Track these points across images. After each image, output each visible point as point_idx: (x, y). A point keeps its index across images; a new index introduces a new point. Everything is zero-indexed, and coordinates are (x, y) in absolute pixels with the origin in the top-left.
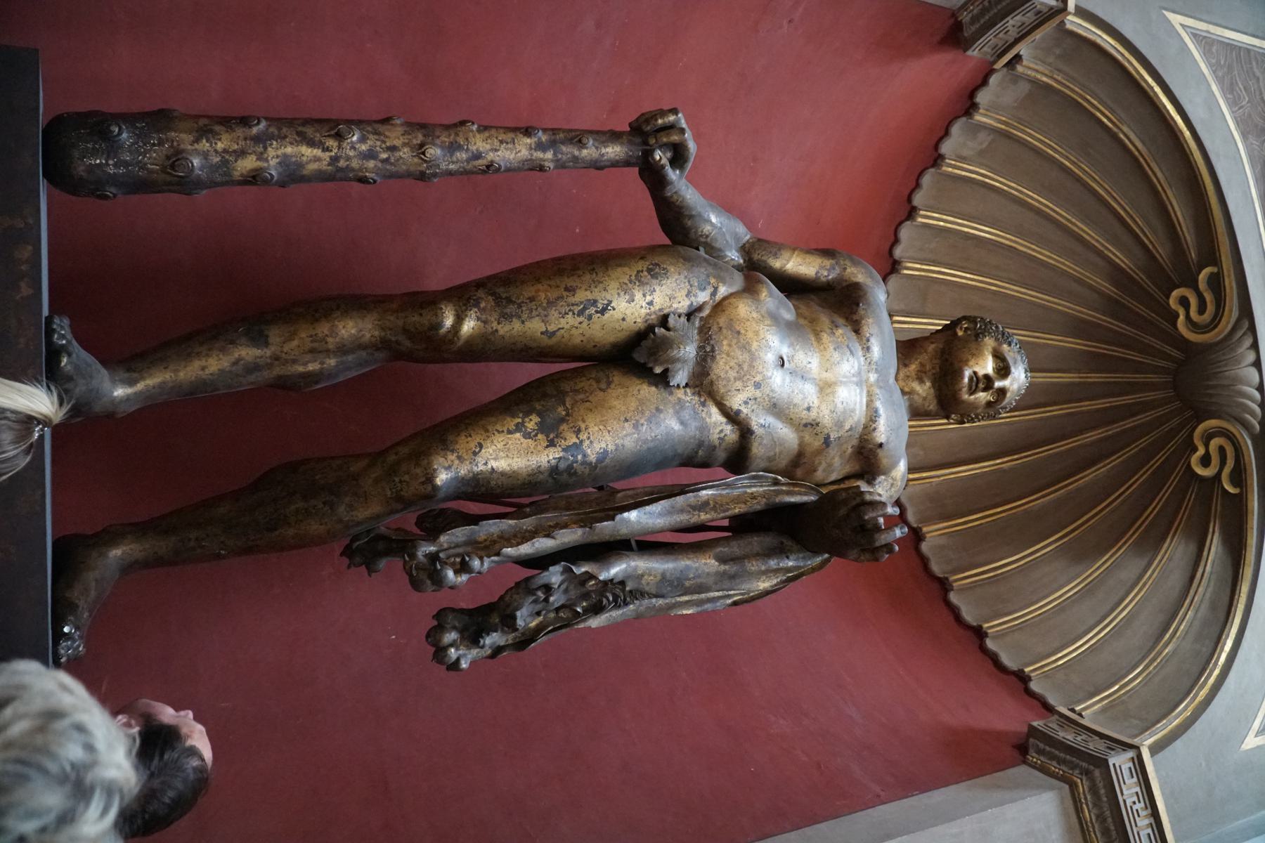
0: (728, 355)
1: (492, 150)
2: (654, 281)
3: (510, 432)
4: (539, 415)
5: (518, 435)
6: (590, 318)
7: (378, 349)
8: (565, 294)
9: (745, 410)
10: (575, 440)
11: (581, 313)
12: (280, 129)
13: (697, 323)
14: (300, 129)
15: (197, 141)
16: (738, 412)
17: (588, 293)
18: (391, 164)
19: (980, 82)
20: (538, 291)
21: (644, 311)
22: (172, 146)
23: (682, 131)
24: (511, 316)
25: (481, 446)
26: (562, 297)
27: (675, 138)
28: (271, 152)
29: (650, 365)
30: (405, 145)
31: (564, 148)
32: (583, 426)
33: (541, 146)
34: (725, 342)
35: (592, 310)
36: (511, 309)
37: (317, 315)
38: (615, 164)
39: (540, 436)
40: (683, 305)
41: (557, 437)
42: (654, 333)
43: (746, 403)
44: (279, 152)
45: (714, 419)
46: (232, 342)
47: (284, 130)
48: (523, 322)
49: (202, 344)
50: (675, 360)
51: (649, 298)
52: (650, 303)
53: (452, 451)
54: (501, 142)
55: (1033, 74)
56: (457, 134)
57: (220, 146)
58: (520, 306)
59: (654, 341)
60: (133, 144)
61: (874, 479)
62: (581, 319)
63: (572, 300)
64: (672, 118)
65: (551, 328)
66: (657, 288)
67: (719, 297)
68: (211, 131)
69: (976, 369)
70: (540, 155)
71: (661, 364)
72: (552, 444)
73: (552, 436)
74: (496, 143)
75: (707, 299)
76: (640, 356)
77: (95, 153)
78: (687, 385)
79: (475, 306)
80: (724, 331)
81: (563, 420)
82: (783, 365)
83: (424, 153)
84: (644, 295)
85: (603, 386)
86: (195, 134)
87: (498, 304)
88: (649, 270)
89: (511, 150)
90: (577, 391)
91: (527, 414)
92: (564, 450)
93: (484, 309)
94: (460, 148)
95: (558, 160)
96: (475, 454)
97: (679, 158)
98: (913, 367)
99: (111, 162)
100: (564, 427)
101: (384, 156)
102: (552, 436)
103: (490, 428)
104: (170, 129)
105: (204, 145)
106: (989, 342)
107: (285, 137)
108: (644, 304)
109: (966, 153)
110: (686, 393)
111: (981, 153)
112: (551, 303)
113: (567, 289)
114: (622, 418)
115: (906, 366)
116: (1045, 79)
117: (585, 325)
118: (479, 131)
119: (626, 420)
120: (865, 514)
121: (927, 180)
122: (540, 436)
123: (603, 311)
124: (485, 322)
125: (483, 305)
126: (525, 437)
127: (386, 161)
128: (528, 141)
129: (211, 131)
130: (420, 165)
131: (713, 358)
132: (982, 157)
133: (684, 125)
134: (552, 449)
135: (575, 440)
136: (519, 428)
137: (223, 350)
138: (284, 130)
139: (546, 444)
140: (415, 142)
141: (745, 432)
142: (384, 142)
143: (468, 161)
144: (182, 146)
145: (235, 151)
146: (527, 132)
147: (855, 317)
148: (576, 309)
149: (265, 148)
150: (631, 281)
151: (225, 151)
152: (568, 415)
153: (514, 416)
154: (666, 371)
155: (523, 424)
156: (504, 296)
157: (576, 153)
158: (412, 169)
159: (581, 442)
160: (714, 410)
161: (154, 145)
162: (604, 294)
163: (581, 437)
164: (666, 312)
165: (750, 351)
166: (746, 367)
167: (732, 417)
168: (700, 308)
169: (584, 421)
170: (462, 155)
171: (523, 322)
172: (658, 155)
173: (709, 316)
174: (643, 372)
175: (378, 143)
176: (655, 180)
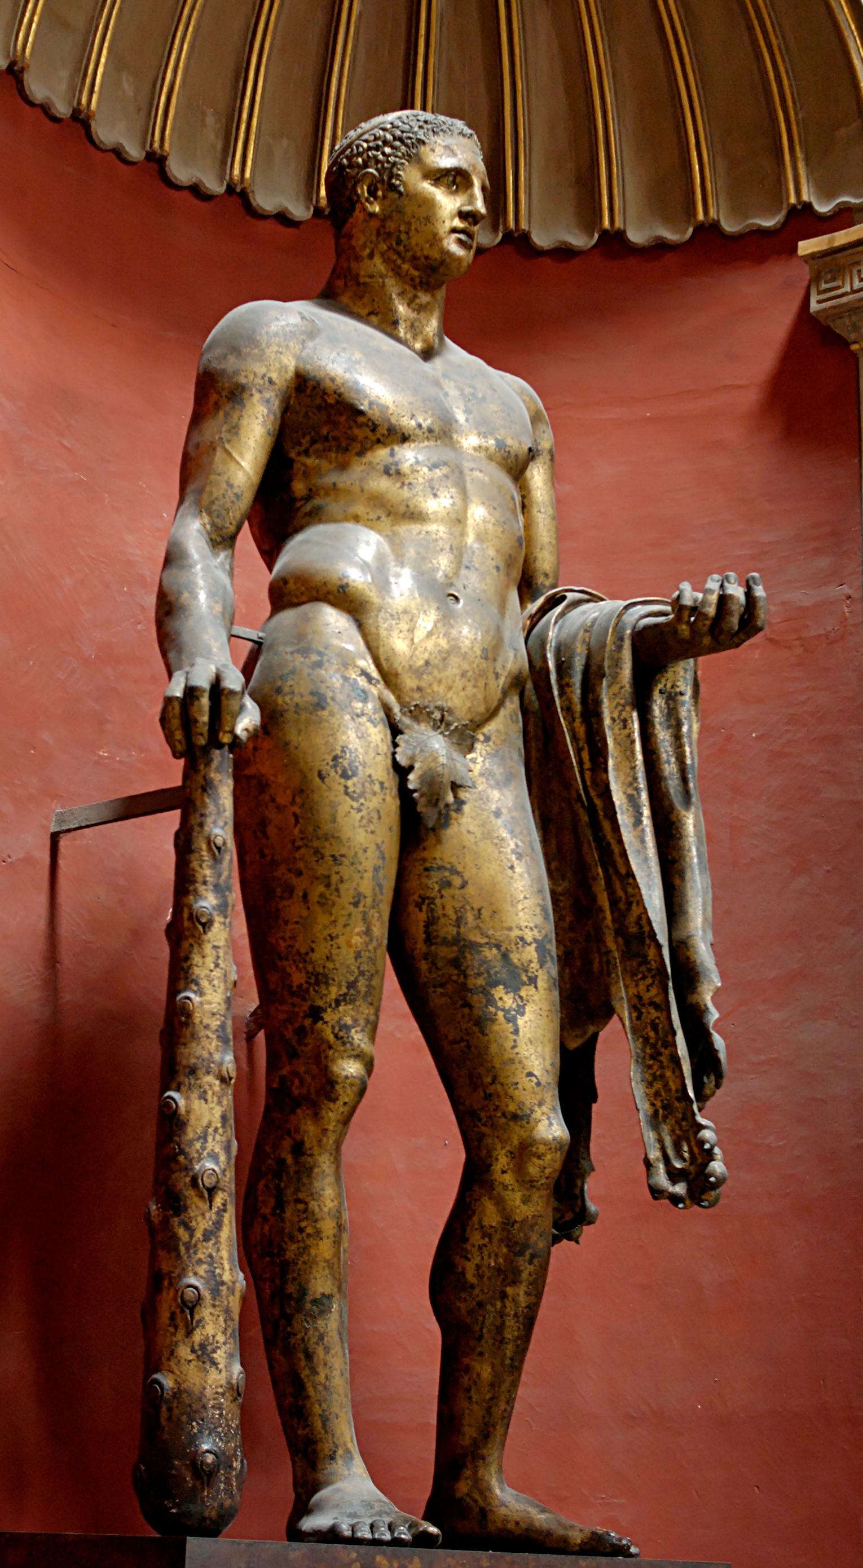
0: (450, 688)
3: (516, 1032)
4: (495, 984)
5: (521, 1021)
8: (361, 908)
9: (502, 681)
12: (200, 1262)
13: (407, 721)
14: (199, 1235)
15: (214, 1364)
20: (349, 945)
21: (388, 799)
22: (223, 1394)
25: (530, 1074)
26: (365, 913)
28: (226, 1277)
30: (220, 1103)
34: (435, 688)
37: (309, 1230)
39: (523, 993)
41: (526, 971)
42: (415, 791)
44: (227, 1266)
45: (501, 727)
46: (321, 1337)
47: (200, 1255)
49: (315, 1372)
51: (377, 788)
52: (382, 784)
53: (532, 1111)
56: (207, 1027)
57: (221, 1338)
59: (422, 796)
60: (221, 1439)
67: (375, 674)
68: (203, 1346)
72: (533, 981)
73: (525, 978)
77: (228, 1482)
80: (423, 684)
81: (505, 956)
82: (457, 598)
85: (457, 881)
86: (208, 1366)
87: (352, 1001)
88: (345, 776)
90: (459, 921)
91: (490, 1001)
93: (355, 1020)
98: (402, 309)
99: (235, 1465)
100: (514, 957)
102: (525, 978)
103: (506, 1056)
104: (202, 1394)
105: (220, 1356)
106: (411, 177)
107: (210, 1256)
113: (356, 904)
114: (510, 872)
115: (395, 323)
119: (512, 867)
120: (731, 628)
122: (523, 993)
125: (348, 1021)
126: (523, 1014)
129: (203, 1346)
131: (450, 711)
137: (327, 1350)
138: (200, 1255)
139: (532, 988)
140: (217, 1088)
142: (216, 1130)
144: (223, 1382)
145: (225, 1321)
147: (382, 431)
149: (223, 1283)
151: (224, 1332)
152: (498, 947)
153: (493, 1021)
156: (344, 990)
161: (221, 1415)
166: (466, 667)
168: (387, 710)
169: (510, 929)
173: (399, 698)
175: (218, 1137)
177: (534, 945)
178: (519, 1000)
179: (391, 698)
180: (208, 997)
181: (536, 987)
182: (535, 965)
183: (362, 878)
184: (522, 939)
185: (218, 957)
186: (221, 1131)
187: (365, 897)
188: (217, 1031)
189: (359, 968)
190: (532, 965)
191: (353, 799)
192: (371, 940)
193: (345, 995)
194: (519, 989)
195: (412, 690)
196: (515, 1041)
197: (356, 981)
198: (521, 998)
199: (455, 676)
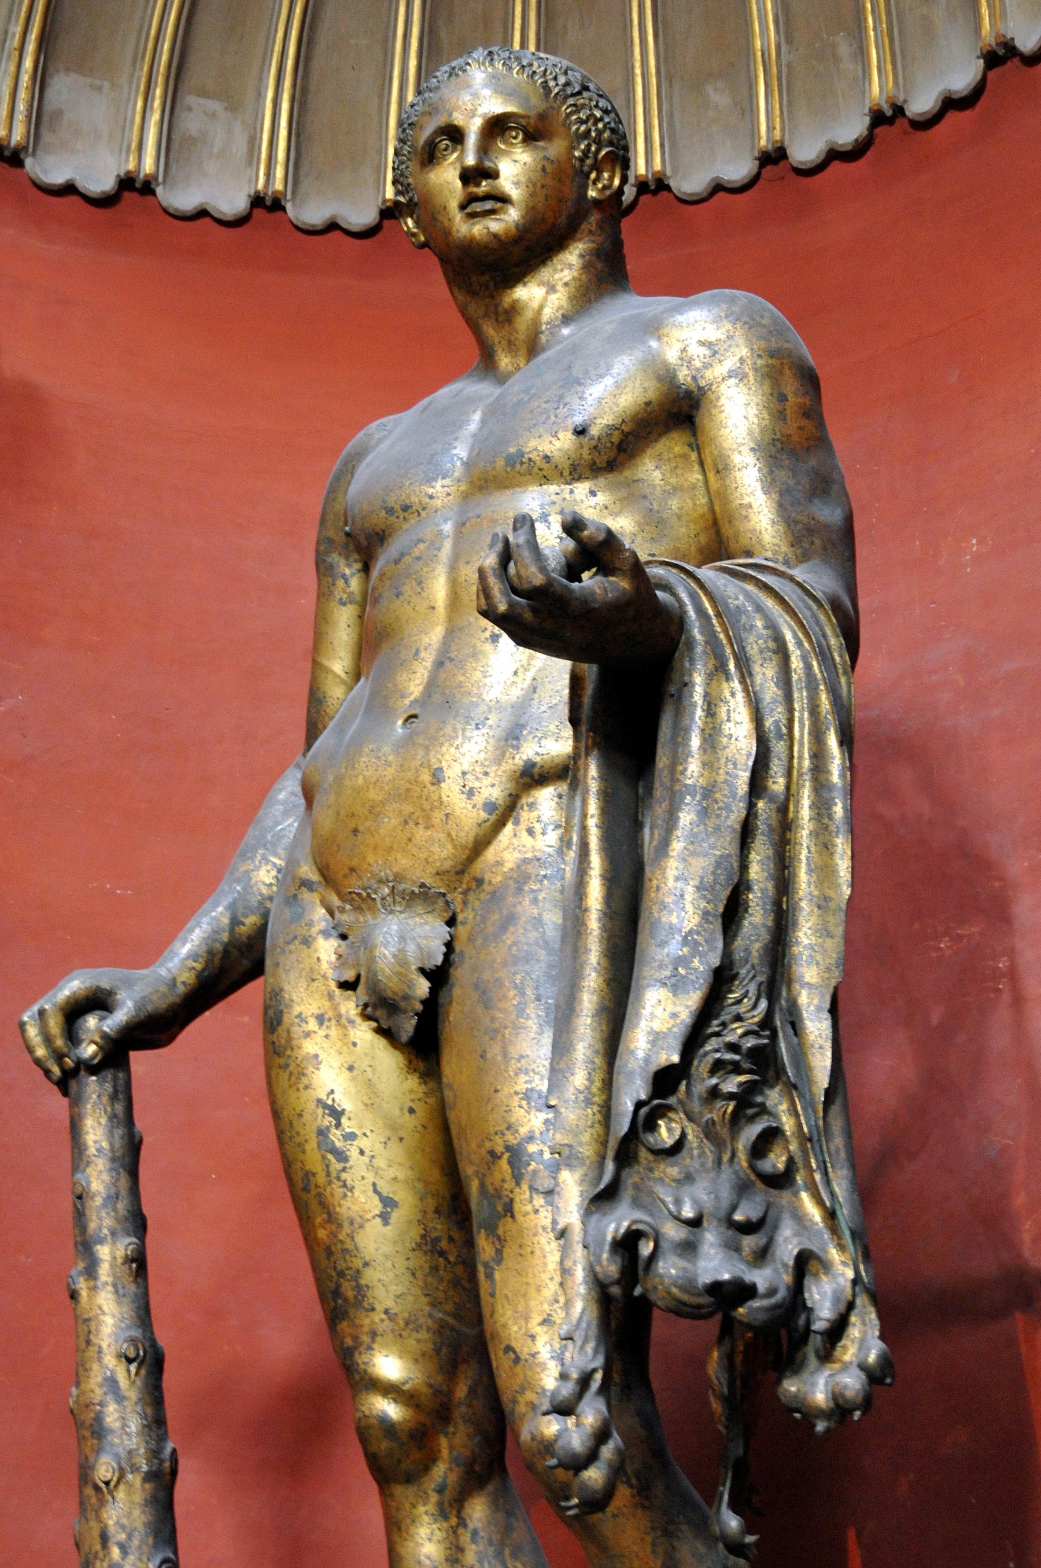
1: (100, 1359)
2: (286, 1019)
5: (497, 1275)
6: (351, 1137)
7: (462, 1523)
10: (504, 1163)
11: (342, 1156)
16: (490, 807)
17: (308, 1147)
18: (130, 1537)
19: (75, 198)
23: (42, 1013)
24: (359, 1287)
25: (509, 1349)
27: (55, 1024)
29: (419, 1007)
31: (92, 1226)
32: (488, 1145)
33: (91, 1272)
35: (336, 1137)
36: (348, 1290)
38: (125, 1120)
40: (327, 949)
41: (500, 1197)
43: (471, 793)
48: (366, 1264)
50: (401, 960)
51: (312, 1025)
52: (320, 1019)
54: (88, 1342)
55: (23, 94)
58: (341, 1274)
59: (375, 1008)
61: (689, 394)
62: (353, 1153)
63: (321, 1179)
64: (32, 1032)
65: (375, 1206)
66: (297, 1009)
69: (454, 205)
70: (104, 1272)
71: (411, 985)
72: (509, 1209)
74: (92, 1352)
75: (315, 898)
76: (408, 1026)
78: (451, 922)
79: (352, 1355)
82: (414, 716)
83: (107, 1483)
84: (307, 1035)
89: (99, 1323)
92: (518, 1184)
94: (99, 1419)
95: (113, 1234)
96: (517, 1360)
97: (98, 1001)
101: (115, 1552)
108: (322, 1033)
109: (240, 145)
110: (464, 923)
111: (234, 106)
112: (332, 1218)
116: (28, 63)
117: (363, 1143)
118: (78, 1384)
121: (311, 212)
122: (500, 1232)
123: (337, 1114)
124: (374, 1334)
127: (124, 1549)
128: (84, 1293)
130: (130, 1485)
131: (398, 878)
132: (236, 98)
133: (35, 1008)
134: (517, 1207)
135: (504, 1163)
136: (490, 1276)
141: (532, 777)
142: (97, 1553)
143: (120, 1398)
146: (74, 1295)
148: (336, 1166)
150: (287, 1066)
154: (422, 971)
155: (486, 1265)
157: (98, 1201)
158: (138, 1498)
159: (508, 1148)
160: (490, 854)
162: (307, 1117)
163: (499, 1149)
164: (333, 985)
165: (383, 803)
167: (505, 812)
170: (112, 1415)
171: (366, 1264)
172: (89, 1050)
173: (339, 894)
174: (431, 1013)
176: (155, 1029)
177: (506, 1156)
178: (497, 1242)
179: (335, 901)
180: (83, 1386)
181: (513, 1217)
182: (509, 1184)
183: (304, 1152)
184: (492, 1153)
185: (89, 1332)
186: (101, 1555)
187: (314, 1174)
188: (91, 1425)
189: (335, 1268)
190: (506, 1186)
191: (279, 1055)
192: (340, 1226)
193: (335, 1308)
194: (496, 1227)
195: (345, 876)
196: (492, 1305)
197: (338, 1286)
198: (499, 1238)
199: (394, 829)
